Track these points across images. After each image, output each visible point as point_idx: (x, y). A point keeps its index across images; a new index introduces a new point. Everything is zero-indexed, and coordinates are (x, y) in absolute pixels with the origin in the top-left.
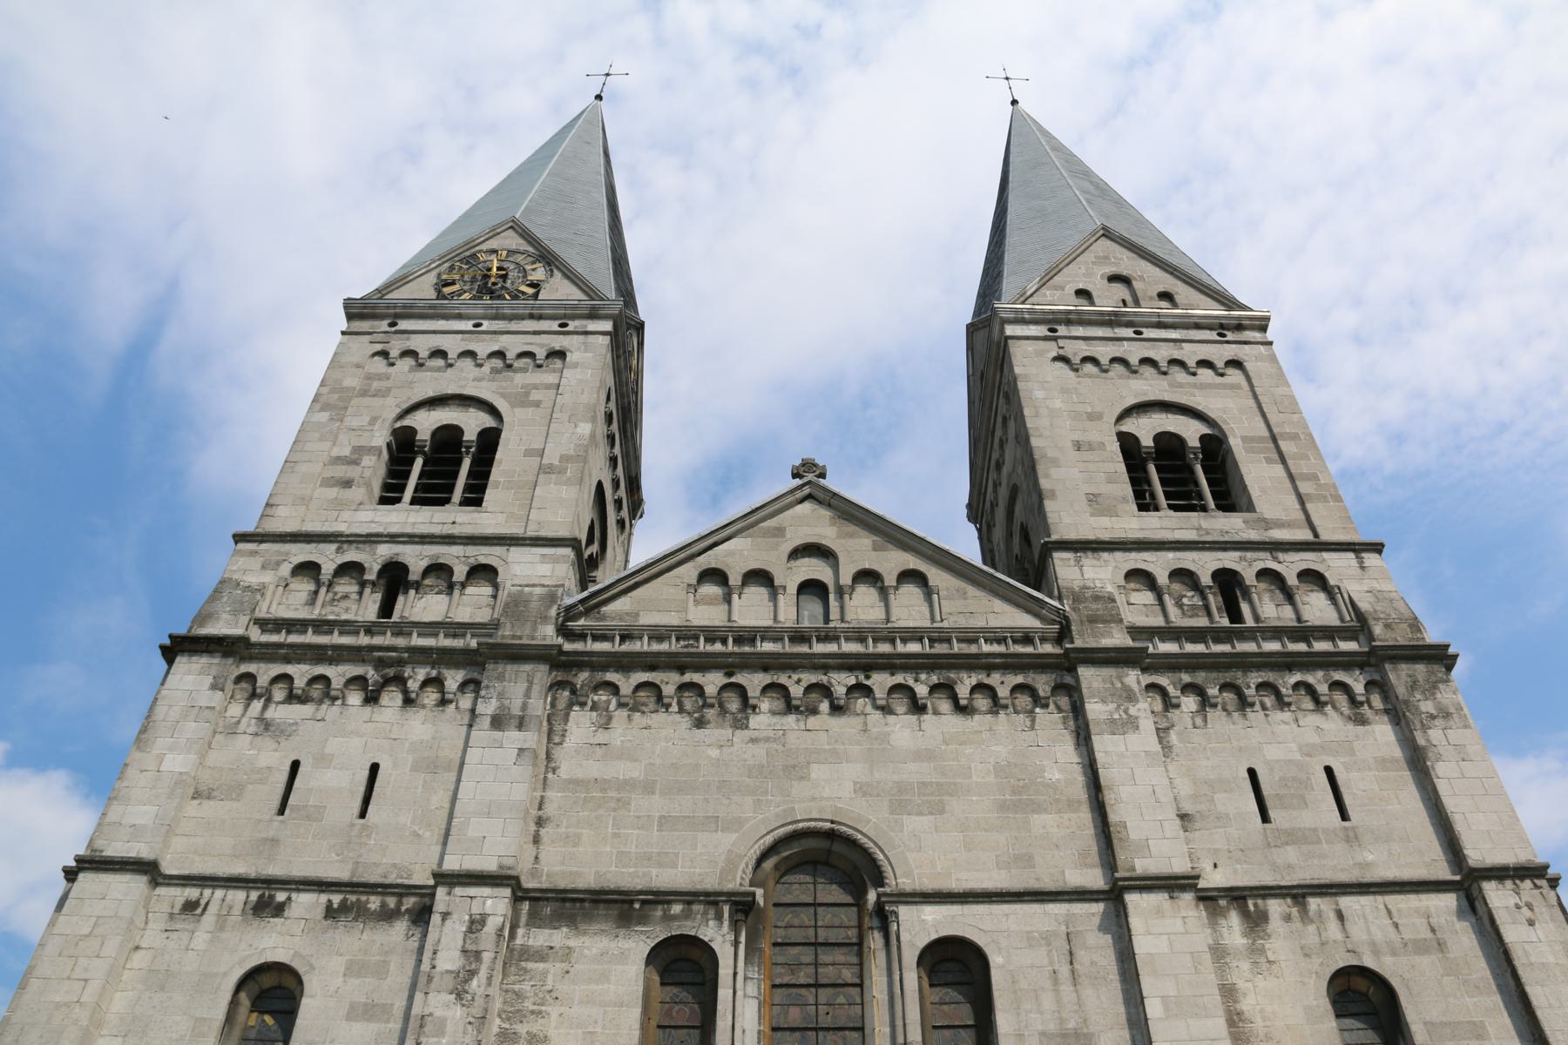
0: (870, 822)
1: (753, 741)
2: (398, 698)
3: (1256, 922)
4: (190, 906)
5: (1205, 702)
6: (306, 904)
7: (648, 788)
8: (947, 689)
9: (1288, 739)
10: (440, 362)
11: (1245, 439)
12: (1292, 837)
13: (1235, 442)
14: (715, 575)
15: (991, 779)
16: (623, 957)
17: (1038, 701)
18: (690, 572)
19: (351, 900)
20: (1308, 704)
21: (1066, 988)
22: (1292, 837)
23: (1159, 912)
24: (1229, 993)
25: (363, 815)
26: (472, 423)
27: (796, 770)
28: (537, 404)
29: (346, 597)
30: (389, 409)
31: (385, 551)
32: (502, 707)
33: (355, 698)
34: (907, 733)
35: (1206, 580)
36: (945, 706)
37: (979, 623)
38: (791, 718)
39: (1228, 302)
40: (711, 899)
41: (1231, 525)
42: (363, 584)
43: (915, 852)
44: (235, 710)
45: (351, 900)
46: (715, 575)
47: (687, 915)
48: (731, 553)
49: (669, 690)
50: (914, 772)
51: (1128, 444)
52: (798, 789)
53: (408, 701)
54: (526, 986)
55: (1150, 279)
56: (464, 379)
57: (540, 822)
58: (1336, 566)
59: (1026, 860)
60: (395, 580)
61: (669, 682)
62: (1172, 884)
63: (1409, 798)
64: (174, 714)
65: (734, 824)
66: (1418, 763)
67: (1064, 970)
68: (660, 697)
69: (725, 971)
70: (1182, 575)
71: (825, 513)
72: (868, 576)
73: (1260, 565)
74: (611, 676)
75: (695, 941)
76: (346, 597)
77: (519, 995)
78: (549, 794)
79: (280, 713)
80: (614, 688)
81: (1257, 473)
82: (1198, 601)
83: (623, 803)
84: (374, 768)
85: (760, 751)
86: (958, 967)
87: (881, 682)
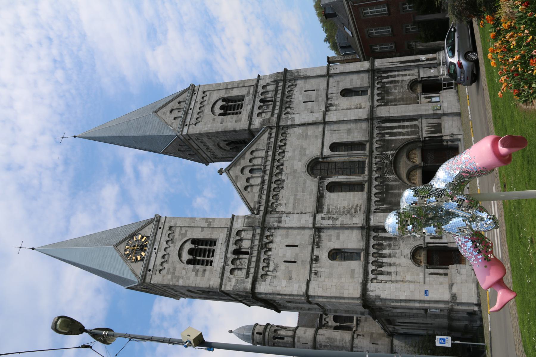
0: (306, 159)
2: (271, 244)
3: (331, 105)
4: (316, 274)
5: (289, 107)
6: (316, 252)
7: (296, 195)
8: (280, 147)
9: (298, 96)
10: (166, 257)
11: (225, 94)
12: (317, 98)
13: (226, 96)
14: (246, 188)
16: (330, 196)
17: (285, 133)
18: (245, 193)
19: (316, 243)
20: (292, 92)
21: (340, 132)
23: (329, 117)
24: (342, 110)
25: (297, 246)
26: (189, 246)
27: (295, 171)
28: (186, 231)
29: (240, 262)
30: (180, 266)
31: (229, 255)
32: (276, 222)
33: (269, 253)
35: (262, 104)
36: (284, 148)
37: (266, 141)
39: (188, 89)
40: (320, 184)
41: (247, 99)
42: (238, 259)
43: (313, 150)
44: (270, 277)
45: (316, 243)
46: (246, 188)
47: (322, 187)
48: (241, 185)
49: (275, 193)
50: (297, 152)
51: (220, 115)
52: (299, 171)
53: (271, 242)
54: (334, 211)
55: (174, 105)
56: (173, 250)
57: (302, 213)
58: (261, 83)
59: (317, 137)
60: (238, 252)
61: (272, 193)
62: (325, 115)
63: (313, 81)
64: (271, 288)
65: (305, 181)
66: (306, 78)
68: (276, 195)
69: (333, 180)
70: (259, 108)
71: (233, 168)
72: (250, 161)
73: (260, 95)
74: (270, 204)
75: (327, 185)
76: (240, 262)
77: (336, 212)
78: (296, 212)
79: (271, 267)
80: (273, 203)
81: (235, 93)
82: (266, 106)
84: (287, 246)
85: (290, 177)
86: (334, 147)
87: (277, 157)
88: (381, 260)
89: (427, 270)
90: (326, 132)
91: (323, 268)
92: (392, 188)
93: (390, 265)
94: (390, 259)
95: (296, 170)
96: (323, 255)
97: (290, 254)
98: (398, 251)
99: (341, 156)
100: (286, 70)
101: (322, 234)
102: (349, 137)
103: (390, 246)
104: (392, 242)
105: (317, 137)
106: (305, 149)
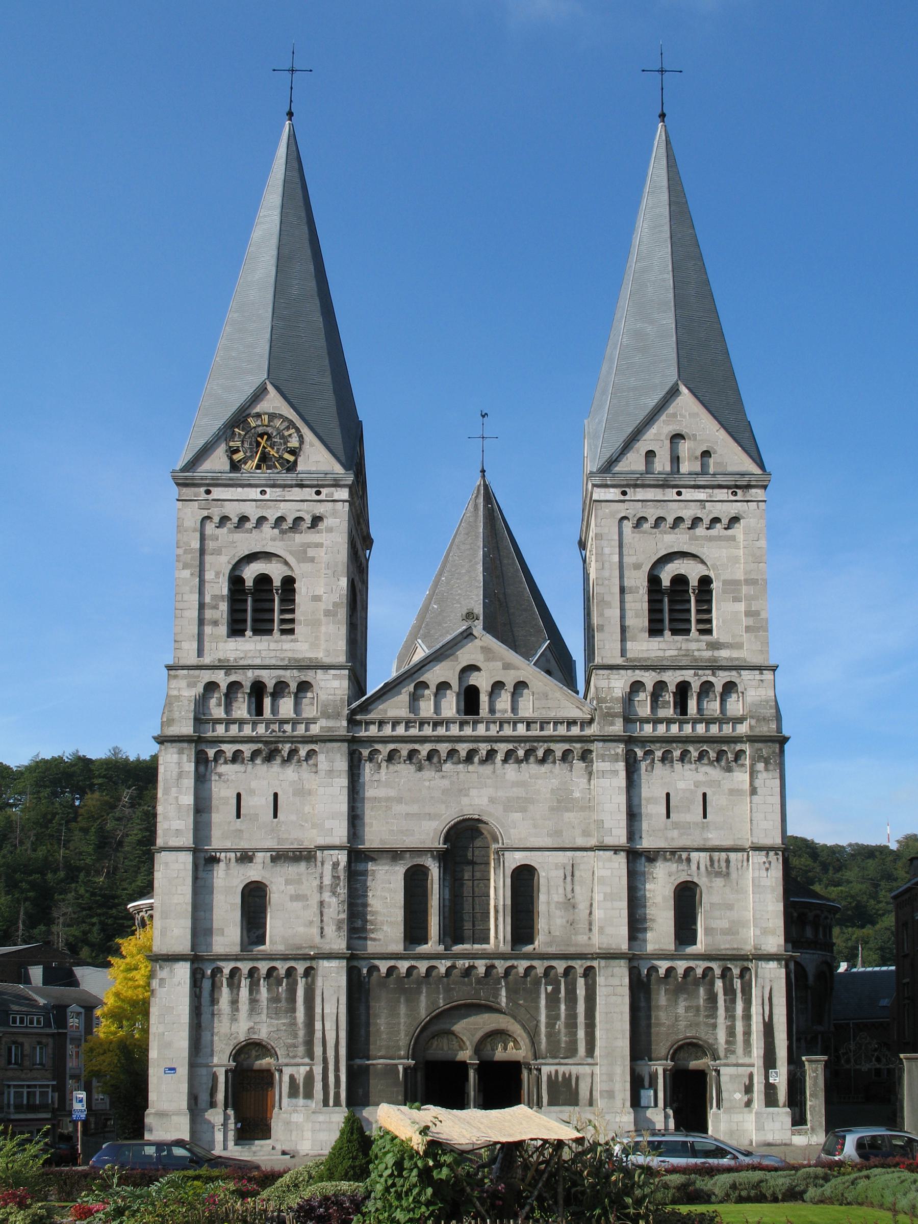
1: (443, 777)
6: (259, 855)
7: (400, 800)
12: (676, 826)
15: (548, 796)
19: (280, 857)
22: (676, 826)
25: (275, 816)
27: (463, 792)
34: (513, 773)
38: (461, 766)
40: (429, 851)
45: (280, 857)
52: (465, 801)
54: (358, 886)
59: (558, 833)
61: (405, 749)
67: (569, 878)
83: (388, 808)
88: (245, 984)
89: (223, 1069)
90: (569, 854)
91: (227, 874)
92: (412, 1001)
93: (234, 1002)
94: (247, 1002)
95: (467, 795)
96: (253, 872)
97: (257, 803)
98: (264, 1017)
99: (499, 892)
100: (785, 740)
101: (303, 865)
102: (553, 906)
103: (274, 1000)
104: (283, 1004)
105: (558, 833)
106: (523, 810)
